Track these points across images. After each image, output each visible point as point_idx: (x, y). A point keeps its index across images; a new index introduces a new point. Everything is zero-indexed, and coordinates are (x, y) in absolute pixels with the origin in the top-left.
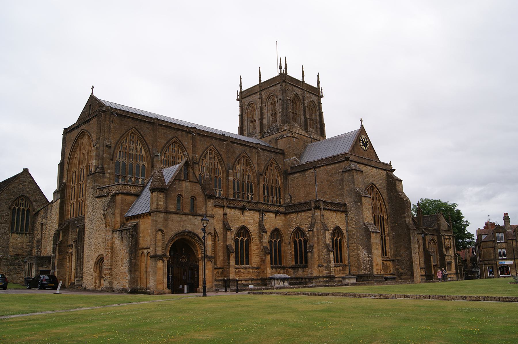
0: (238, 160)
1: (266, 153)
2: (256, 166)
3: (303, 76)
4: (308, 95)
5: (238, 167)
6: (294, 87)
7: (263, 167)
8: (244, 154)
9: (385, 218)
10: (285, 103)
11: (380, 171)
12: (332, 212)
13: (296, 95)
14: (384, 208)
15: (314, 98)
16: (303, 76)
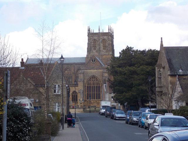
0: (66, 70)
1: (77, 65)
2: (73, 70)
3: (99, 30)
4: (102, 37)
5: (66, 72)
6: (94, 37)
7: (76, 70)
8: (68, 67)
9: (101, 86)
10: (100, 41)
11: (99, 70)
12: (73, 87)
13: (95, 40)
14: (100, 82)
15: (105, 37)
16: (99, 30)
